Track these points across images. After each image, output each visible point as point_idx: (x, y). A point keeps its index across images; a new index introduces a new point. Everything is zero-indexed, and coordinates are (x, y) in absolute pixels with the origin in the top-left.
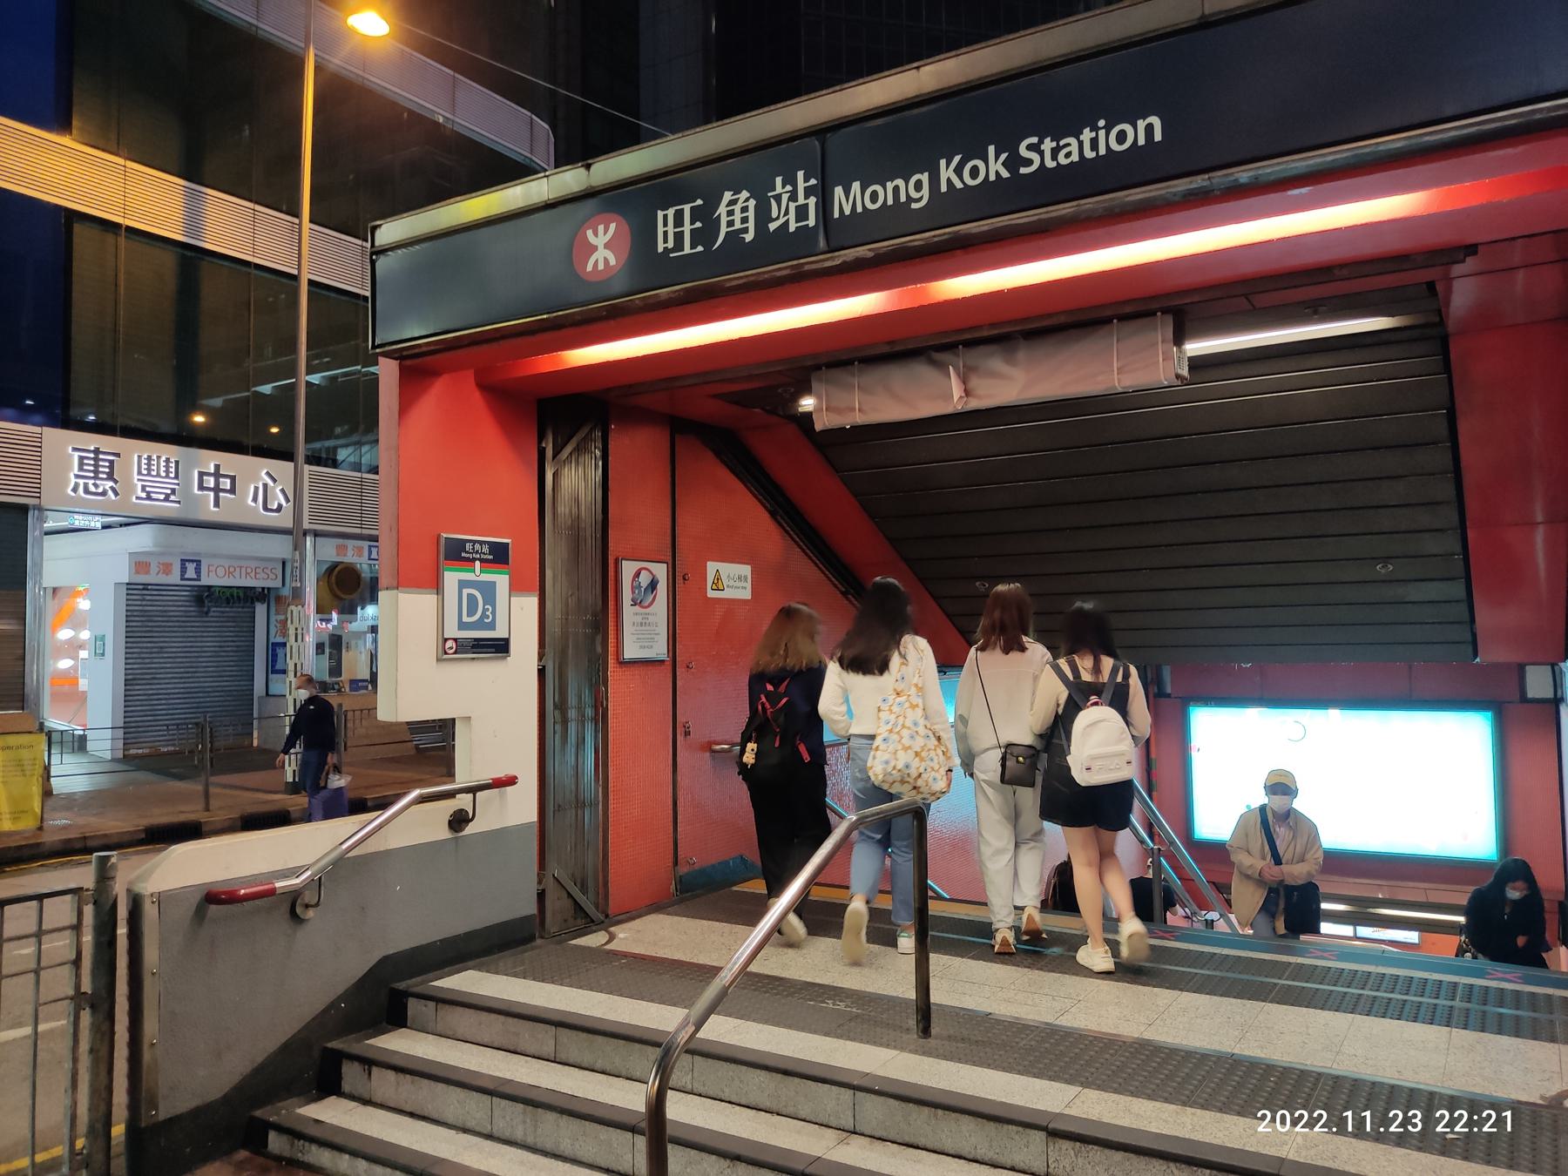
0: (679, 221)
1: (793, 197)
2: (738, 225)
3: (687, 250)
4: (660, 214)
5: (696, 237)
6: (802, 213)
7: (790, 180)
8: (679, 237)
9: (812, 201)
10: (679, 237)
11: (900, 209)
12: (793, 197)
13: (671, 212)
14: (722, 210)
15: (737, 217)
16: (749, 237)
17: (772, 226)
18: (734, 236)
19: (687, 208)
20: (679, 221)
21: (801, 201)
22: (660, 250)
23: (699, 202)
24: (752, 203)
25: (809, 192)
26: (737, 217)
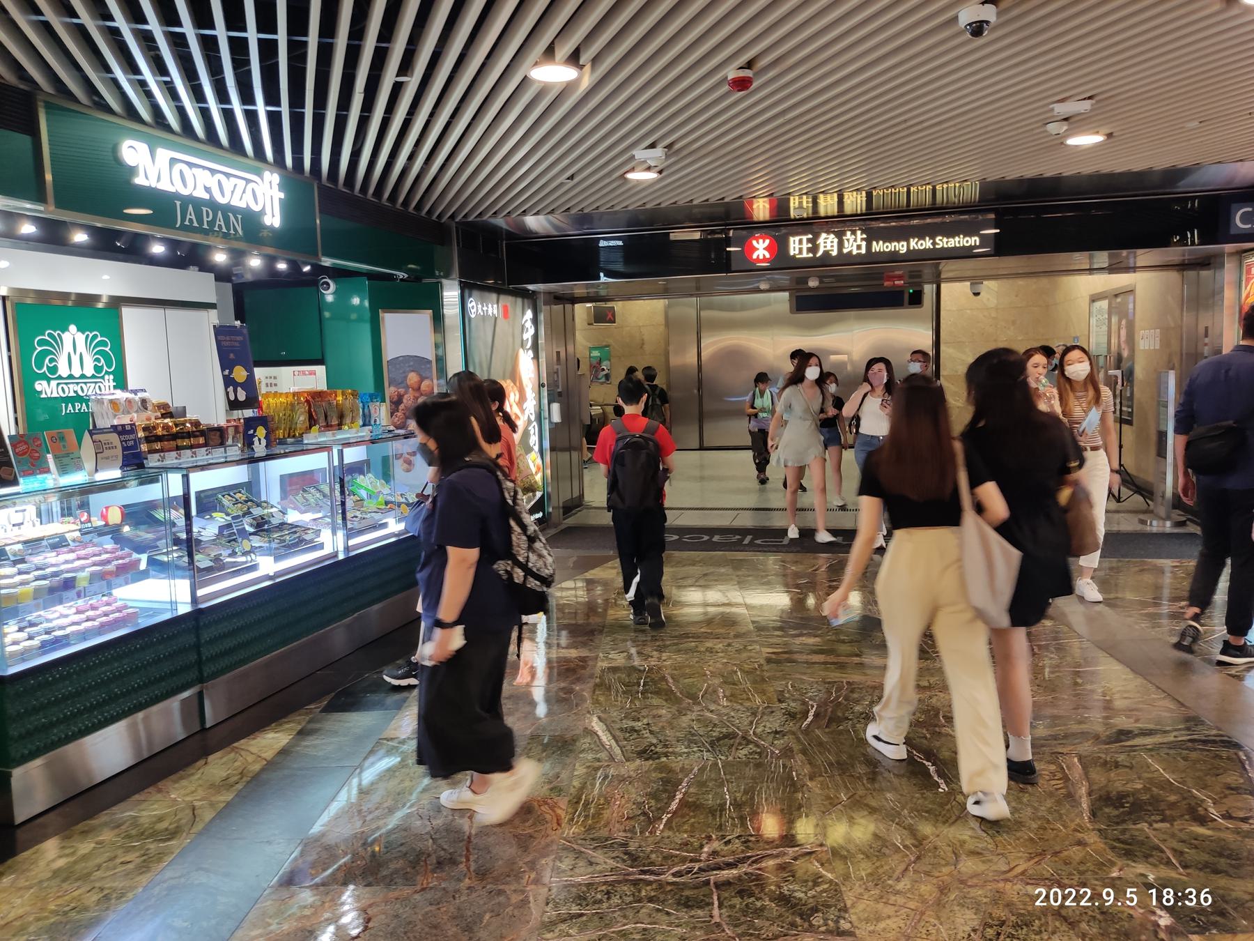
0: (801, 242)
1: (855, 240)
2: (829, 248)
3: (805, 255)
4: (792, 239)
5: (809, 250)
6: (859, 247)
7: (854, 233)
8: (801, 250)
9: (864, 244)
10: (801, 250)
11: (895, 253)
12: (855, 240)
13: (797, 239)
14: (821, 241)
15: (829, 245)
16: (834, 253)
17: (845, 251)
18: (826, 253)
19: (804, 238)
20: (801, 242)
21: (859, 242)
22: (792, 253)
23: (810, 236)
24: (836, 240)
25: (862, 239)
26: (829, 245)
